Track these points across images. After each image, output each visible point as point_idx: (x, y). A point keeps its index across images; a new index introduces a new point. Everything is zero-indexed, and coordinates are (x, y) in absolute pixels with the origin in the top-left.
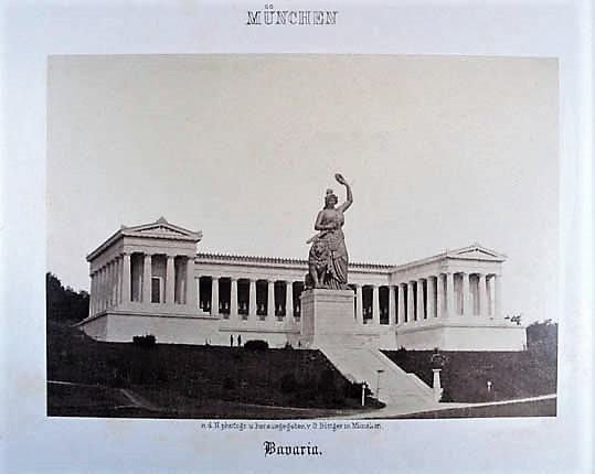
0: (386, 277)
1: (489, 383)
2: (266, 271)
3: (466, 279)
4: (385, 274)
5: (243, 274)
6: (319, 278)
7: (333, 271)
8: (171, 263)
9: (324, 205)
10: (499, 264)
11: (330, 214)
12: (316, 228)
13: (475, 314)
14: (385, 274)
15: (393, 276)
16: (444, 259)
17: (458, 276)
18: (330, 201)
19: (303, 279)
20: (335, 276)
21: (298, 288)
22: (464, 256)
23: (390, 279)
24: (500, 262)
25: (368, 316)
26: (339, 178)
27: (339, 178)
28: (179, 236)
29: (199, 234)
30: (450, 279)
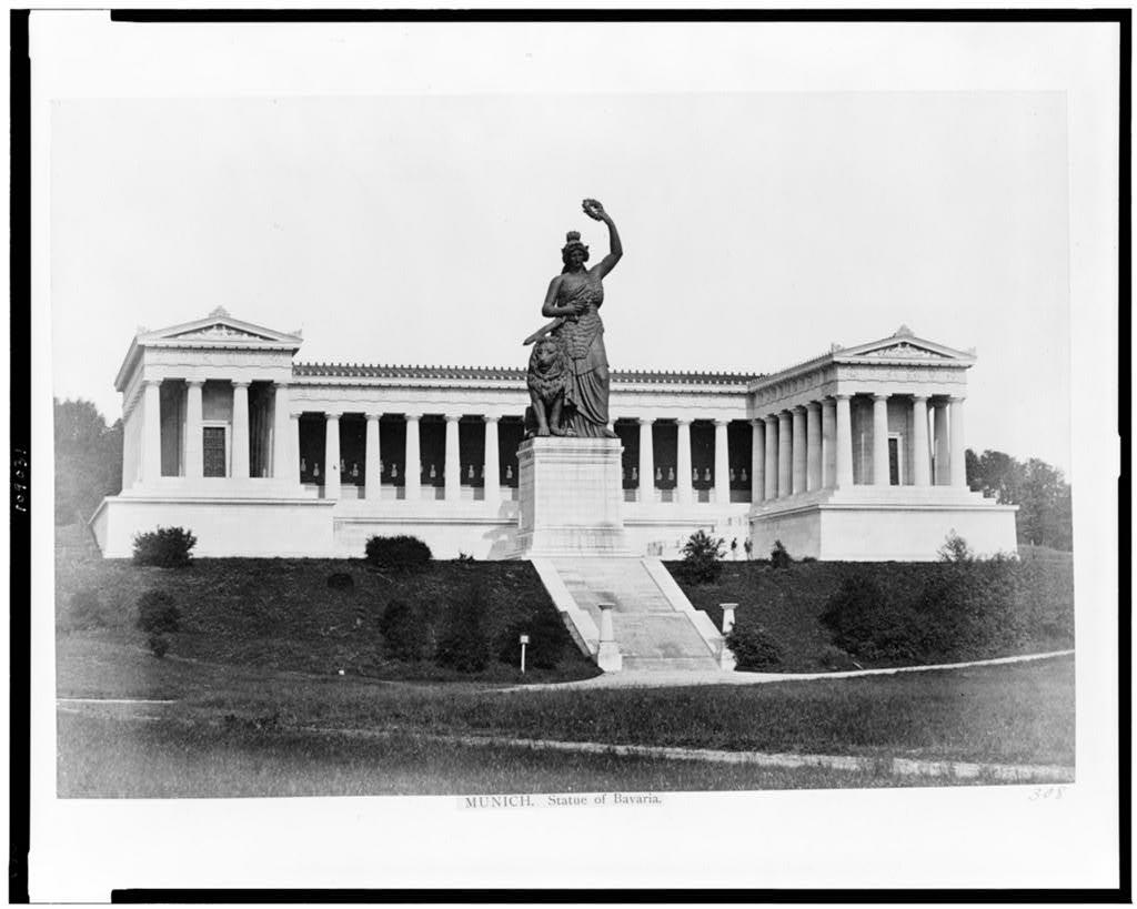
0: (742, 402)
1: (525, 639)
2: (478, 396)
3: (881, 409)
4: (739, 394)
5: (433, 404)
6: (548, 416)
8: (241, 398)
9: (563, 265)
10: (957, 375)
11: (575, 282)
12: (546, 313)
13: (892, 484)
14: (739, 394)
15: (758, 401)
16: (827, 367)
17: (863, 403)
18: (574, 254)
19: (520, 411)
20: (580, 409)
22: (874, 358)
23: (751, 406)
25: (630, 484)
26: (593, 209)
27: (593, 209)
28: (256, 343)
29: (294, 337)
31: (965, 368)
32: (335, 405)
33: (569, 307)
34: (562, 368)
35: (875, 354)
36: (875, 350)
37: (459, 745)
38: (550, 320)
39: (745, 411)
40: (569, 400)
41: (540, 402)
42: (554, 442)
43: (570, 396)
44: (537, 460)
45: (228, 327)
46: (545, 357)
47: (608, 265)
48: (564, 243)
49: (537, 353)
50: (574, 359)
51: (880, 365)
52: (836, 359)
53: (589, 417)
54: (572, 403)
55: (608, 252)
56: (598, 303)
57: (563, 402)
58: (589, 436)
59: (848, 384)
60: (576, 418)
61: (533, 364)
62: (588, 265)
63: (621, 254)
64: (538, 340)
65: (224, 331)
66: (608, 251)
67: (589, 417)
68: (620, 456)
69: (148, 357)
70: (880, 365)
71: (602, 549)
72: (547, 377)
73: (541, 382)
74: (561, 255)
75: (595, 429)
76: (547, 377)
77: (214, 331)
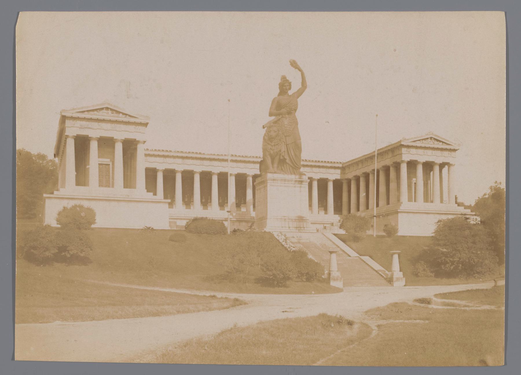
0: (339, 171)
3: (420, 169)
5: (206, 167)
6: (273, 163)
7: (287, 157)
8: (119, 148)
9: (278, 91)
10: (453, 153)
12: (271, 115)
15: (347, 171)
16: (399, 146)
17: (412, 165)
20: (288, 161)
21: (255, 177)
22: (418, 144)
24: (455, 150)
26: (294, 64)
27: (294, 64)
30: (404, 168)
31: (457, 150)
32: (161, 165)
33: (283, 110)
34: (280, 140)
35: (419, 142)
36: (419, 140)
37: (333, 354)
38: (273, 118)
39: (339, 175)
40: (283, 156)
41: (269, 157)
42: (276, 176)
43: (283, 154)
44: (268, 185)
45: (111, 110)
46: (273, 134)
47: (300, 93)
48: (279, 81)
49: (268, 132)
50: (285, 136)
51: (421, 148)
52: (402, 143)
53: (292, 165)
54: (284, 158)
55: (300, 86)
56: (295, 110)
57: (280, 156)
58: (291, 174)
59: (407, 156)
60: (285, 165)
61: (266, 138)
62: (290, 93)
63: (306, 87)
64: (268, 127)
65: (110, 112)
66: (300, 86)
67: (292, 165)
68: (307, 184)
69: (68, 123)
70: (421, 148)
71: (300, 229)
72: (273, 144)
73: (269, 147)
74: (278, 86)
75: (295, 170)
76: (273, 144)
77: (104, 111)
